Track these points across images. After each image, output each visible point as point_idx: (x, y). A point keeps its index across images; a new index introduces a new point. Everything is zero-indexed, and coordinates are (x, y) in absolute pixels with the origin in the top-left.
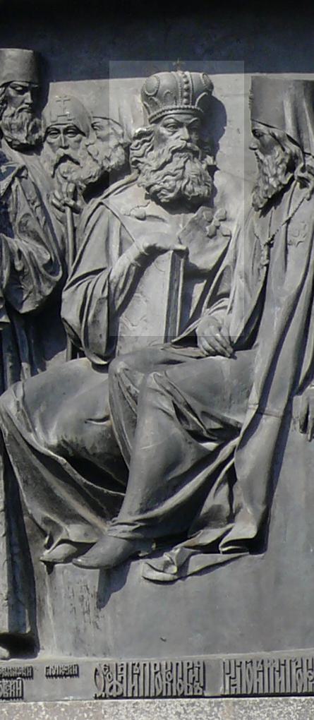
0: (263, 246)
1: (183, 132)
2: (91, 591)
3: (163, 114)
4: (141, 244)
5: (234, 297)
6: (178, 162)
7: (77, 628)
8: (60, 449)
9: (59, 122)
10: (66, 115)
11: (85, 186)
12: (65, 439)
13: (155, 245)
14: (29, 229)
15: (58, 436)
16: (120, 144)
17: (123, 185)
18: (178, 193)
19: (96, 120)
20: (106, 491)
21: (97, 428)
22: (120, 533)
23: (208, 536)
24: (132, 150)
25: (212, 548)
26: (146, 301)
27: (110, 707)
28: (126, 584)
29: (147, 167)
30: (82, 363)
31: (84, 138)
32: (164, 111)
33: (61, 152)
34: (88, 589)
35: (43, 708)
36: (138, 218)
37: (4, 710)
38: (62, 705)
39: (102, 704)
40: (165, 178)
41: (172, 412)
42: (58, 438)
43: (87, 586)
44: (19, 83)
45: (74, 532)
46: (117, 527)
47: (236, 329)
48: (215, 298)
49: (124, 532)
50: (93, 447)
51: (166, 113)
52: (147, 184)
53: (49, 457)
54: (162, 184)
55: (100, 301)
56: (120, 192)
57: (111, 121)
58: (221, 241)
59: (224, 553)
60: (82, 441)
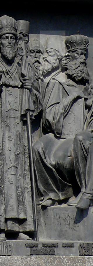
2: (71, 217)
3: (77, 49)
7: (61, 230)
8: (54, 166)
9: (35, 48)
10: (38, 46)
11: (46, 72)
12: (58, 162)
13: (79, 95)
14: (34, 86)
15: (56, 161)
16: (58, 58)
17: (57, 73)
19: (48, 49)
20: (64, 182)
21: (68, 159)
22: (88, 197)
24: (63, 61)
26: (74, 115)
27: (87, 259)
28: (88, 215)
30: (51, 135)
31: (42, 55)
32: (78, 48)
33: (36, 59)
34: (69, 216)
35: (65, 258)
36: (67, 85)
37: (52, 258)
38: (71, 258)
39: (85, 257)
40: (78, 72)
42: (56, 162)
43: (69, 215)
44: (25, 33)
45: (52, 195)
46: (87, 195)
49: (89, 196)
50: (67, 166)
53: (49, 167)
55: (61, 114)
56: (57, 75)
57: (55, 50)
60: (64, 163)
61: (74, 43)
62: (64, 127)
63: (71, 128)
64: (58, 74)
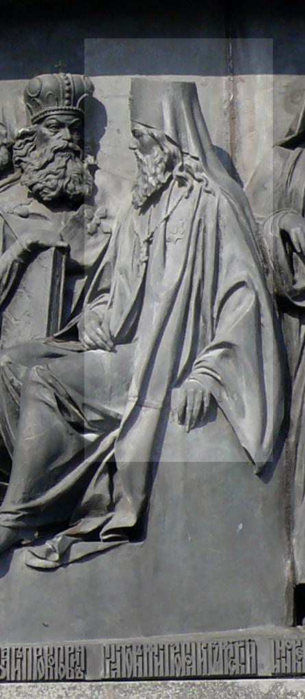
0: (142, 243)
1: (65, 133)
3: (46, 115)
4: (24, 241)
5: (114, 290)
6: (60, 161)
13: (37, 242)
16: (5, 145)
17: (8, 183)
18: (59, 191)
23: (89, 524)
25: (93, 536)
26: (29, 296)
28: (10, 571)
29: (30, 167)
32: (46, 112)
36: (21, 216)
40: (48, 177)
41: (54, 404)
47: (116, 325)
48: (96, 293)
49: (7, 520)
51: (48, 114)
52: (30, 183)
54: (44, 182)
58: (101, 238)
59: (105, 541)
61: (35, 97)
62: (4, 330)
63: (20, 332)
64: (9, 187)
